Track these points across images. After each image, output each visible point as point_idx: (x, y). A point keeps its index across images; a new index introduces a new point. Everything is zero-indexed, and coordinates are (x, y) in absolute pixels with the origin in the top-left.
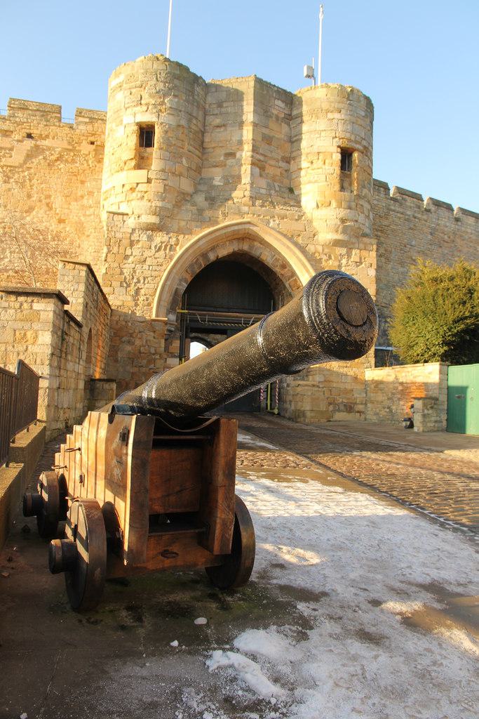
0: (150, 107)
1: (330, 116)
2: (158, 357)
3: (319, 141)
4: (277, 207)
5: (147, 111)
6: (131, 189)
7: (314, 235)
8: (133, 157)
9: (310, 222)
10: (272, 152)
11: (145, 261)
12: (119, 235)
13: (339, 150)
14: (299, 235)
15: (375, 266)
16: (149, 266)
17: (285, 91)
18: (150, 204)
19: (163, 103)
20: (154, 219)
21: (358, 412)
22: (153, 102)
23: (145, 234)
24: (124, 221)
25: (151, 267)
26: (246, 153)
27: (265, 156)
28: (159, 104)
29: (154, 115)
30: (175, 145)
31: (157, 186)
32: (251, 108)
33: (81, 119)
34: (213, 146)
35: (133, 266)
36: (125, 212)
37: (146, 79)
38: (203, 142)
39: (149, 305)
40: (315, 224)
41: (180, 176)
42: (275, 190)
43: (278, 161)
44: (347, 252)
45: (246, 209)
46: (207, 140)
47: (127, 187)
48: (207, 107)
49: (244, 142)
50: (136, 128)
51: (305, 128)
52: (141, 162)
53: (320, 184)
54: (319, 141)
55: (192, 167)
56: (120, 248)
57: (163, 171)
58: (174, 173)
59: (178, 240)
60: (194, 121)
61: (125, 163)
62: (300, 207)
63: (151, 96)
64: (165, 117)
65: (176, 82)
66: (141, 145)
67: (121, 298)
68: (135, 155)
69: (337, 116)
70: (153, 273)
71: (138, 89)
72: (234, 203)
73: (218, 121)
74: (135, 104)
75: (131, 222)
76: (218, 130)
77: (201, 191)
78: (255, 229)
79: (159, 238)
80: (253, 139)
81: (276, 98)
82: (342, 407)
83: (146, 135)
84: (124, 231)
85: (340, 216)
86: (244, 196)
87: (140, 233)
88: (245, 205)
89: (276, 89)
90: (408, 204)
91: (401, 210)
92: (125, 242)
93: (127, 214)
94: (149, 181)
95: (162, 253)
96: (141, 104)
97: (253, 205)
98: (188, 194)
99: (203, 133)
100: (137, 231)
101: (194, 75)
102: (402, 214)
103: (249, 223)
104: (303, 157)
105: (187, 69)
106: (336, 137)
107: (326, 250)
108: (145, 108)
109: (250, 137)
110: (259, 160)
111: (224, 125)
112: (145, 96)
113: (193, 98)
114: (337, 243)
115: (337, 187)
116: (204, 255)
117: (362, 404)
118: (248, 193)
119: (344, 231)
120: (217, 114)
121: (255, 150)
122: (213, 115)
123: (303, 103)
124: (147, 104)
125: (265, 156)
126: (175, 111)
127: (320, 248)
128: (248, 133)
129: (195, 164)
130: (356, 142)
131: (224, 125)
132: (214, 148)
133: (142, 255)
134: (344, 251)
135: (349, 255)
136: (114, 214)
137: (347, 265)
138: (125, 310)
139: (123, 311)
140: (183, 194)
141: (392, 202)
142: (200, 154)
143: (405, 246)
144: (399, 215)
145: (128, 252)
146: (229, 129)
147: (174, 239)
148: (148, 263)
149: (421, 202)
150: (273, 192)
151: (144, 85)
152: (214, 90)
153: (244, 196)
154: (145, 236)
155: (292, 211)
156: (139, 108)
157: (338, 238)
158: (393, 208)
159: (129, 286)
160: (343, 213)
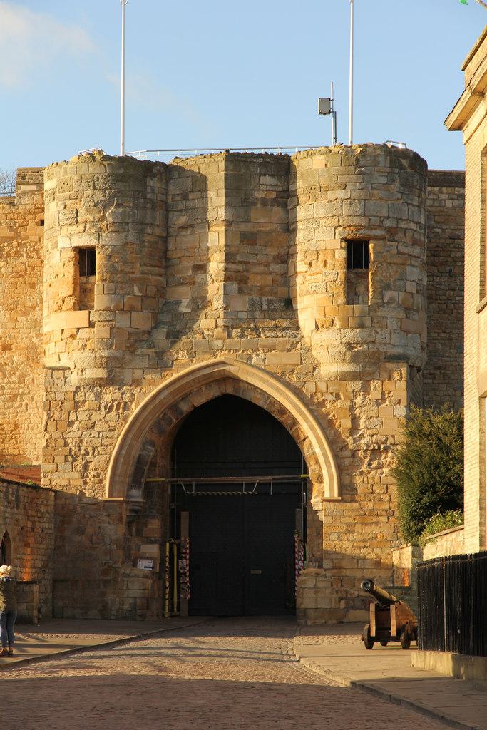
0: (88, 226)
1: (331, 195)
3: (319, 234)
4: (262, 335)
5: (84, 231)
6: (71, 336)
7: (314, 369)
8: (71, 293)
9: (308, 350)
10: (257, 255)
11: (93, 426)
12: (60, 397)
13: (344, 244)
14: (293, 371)
15: (404, 402)
16: (99, 432)
19: (103, 218)
20: (101, 373)
22: (91, 219)
23: (92, 391)
24: (66, 378)
25: (101, 434)
26: (216, 265)
28: (99, 221)
29: (92, 238)
30: (121, 271)
31: (101, 331)
32: (221, 201)
33: (24, 188)
34: (179, 255)
35: (79, 433)
36: (66, 365)
37: (81, 188)
38: (166, 251)
39: (101, 482)
40: (314, 353)
43: (267, 265)
45: (219, 343)
46: (171, 247)
47: (67, 334)
48: (170, 199)
49: (212, 249)
50: (72, 254)
51: (301, 213)
52: (82, 299)
53: (319, 296)
54: (319, 234)
55: (149, 293)
56: (63, 412)
57: (108, 309)
58: (121, 310)
59: (133, 395)
60: (149, 230)
61: (63, 301)
62: (298, 328)
63: (88, 211)
64: (108, 238)
65: (119, 185)
66: (82, 274)
67: (66, 476)
68: (74, 290)
69: (340, 194)
70: (105, 442)
71: (73, 201)
72: (203, 338)
73: (183, 220)
74: (70, 222)
75: (74, 378)
77: (164, 323)
78: (227, 368)
79: (110, 395)
80: (226, 245)
81: (261, 175)
83: (85, 258)
85: (345, 340)
86: (217, 326)
87: (86, 390)
88: (218, 339)
89: (261, 160)
92: (69, 405)
93: (69, 369)
94: (91, 325)
95: (114, 413)
96: (77, 222)
97: (229, 336)
99: (165, 240)
100: (82, 388)
103: (222, 363)
104: (299, 257)
106: (340, 226)
107: (332, 388)
108: (82, 228)
109: (222, 242)
111: (191, 226)
112: (82, 211)
114: (344, 377)
116: (174, 407)
118: (221, 322)
119: (355, 359)
120: (181, 211)
121: (229, 258)
122: (177, 211)
123: (298, 175)
124: (85, 222)
126: (120, 226)
127: (322, 386)
128: (216, 238)
130: (370, 227)
131: (191, 226)
132: (180, 258)
133: (90, 419)
134: (358, 385)
135: (366, 390)
136: (53, 369)
137: (363, 405)
138: (72, 491)
139: (71, 492)
140: (137, 334)
142: (162, 271)
145: (73, 417)
147: (129, 395)
148: (97, 429)
150: (258, 313)
151: (79, 197)
152: (176, 174)
153: (217, 326)
154: (92, 394)
155: (285, 338)
156: (74, 228)
157: (345, 370)
159: (75, 460)
160: (350, 334)
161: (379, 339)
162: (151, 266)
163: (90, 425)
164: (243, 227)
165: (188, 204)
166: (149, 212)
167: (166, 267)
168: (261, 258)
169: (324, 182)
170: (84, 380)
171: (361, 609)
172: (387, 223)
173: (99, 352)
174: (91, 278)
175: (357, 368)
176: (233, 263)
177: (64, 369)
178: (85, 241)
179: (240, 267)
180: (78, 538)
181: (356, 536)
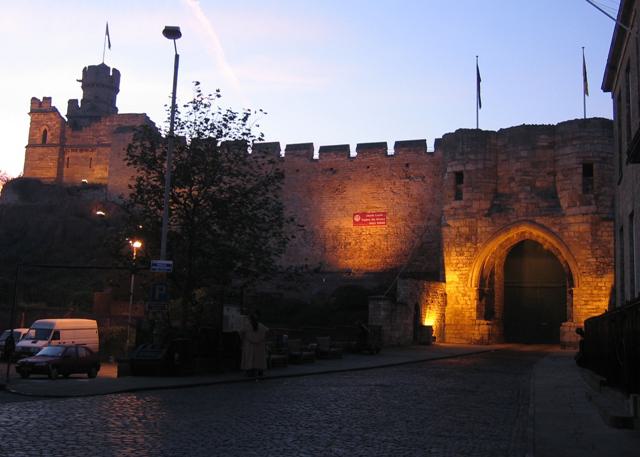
1: (574, 142)
172: (601, 155)
174: (463, 185)
178: (459, 168)
181: (589, 307)
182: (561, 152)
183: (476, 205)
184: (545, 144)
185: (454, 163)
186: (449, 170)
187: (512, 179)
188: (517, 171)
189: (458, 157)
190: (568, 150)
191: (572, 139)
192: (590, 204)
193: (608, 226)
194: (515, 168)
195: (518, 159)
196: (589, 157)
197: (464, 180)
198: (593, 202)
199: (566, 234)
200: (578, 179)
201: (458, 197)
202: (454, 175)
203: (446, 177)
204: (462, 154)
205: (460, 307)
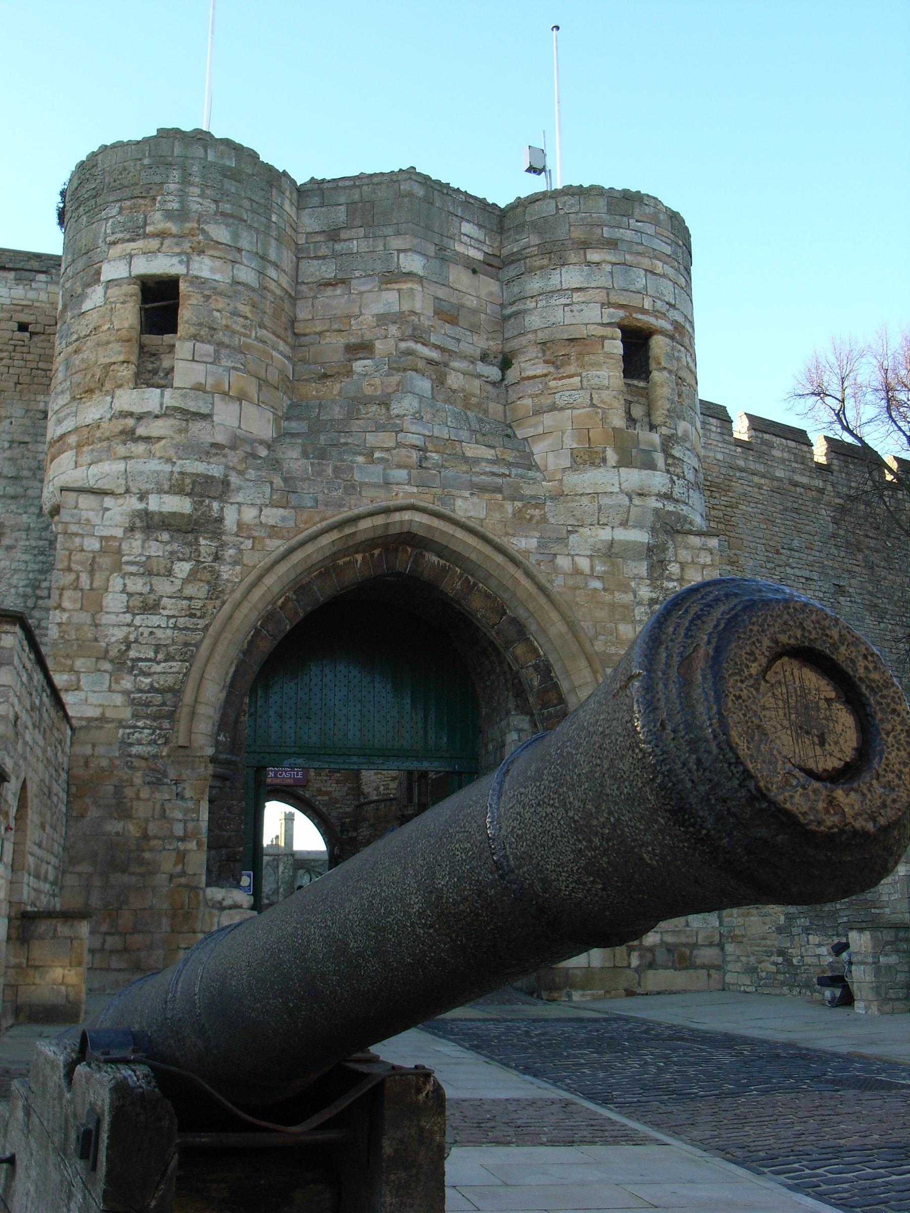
1: (594, 256)
2: (193, 845)
16: (169, 617)
17: (483, 202)
18: (167, 468)
21: (703, 967)
27: (443, 350)
29: (175, 260)
34: (318, 329)
38: (293, 321)
41: (240, 400)
42: (470, 429)
44: (651, 568)
45: (402, 474)
55: (269, 377)
56: (97, 575)
58: (226, 394)
63: (169, 215)
66: (142, 333)
76: (329, 291)
82: (661, 956)
84: (106, 533)
88: (399, 466)
90: (776, 453)
91: (761, 468)
98: (262, 442)
99: (294, 300)
101: (270, 169)
102: (763, 476)
105: (253, 156)
107: (599, 568)
110: (430, 362)
111: (343, 281)
113: (269, 219)
115: (618, 420)
117: (711, 945)
120: (324, 258)
122: (317, 258)
125: (443, 350)
127: (584, 564)
129: (277, 372)
131: (343, 281)
132: (320, 334)
141: (739, 450)
143: (778, 553)
144: (756, 479)
146: (357, 286)
149: (805, 448)
150: (464, 434)
158: (741, 463)
161: (678, 491)
162: (274, 333)
163: (151, 601)
164: (441, 292)
165: (338, 247)
166: (273, 242)
167: (293, 347)
168: (465, 348)
169: (577, 234)
170: (146, 514)
171: (666, 968)
173: (179, 462)
174: (167, 338)
175: (641, 536)
176: (424, 344)
177: (101, 493)
178: (163, 265)
179: (435, 355)
180: (114, 826)
182: (534, 284)
183: (226, 414)
184: (473, 253)
185: (140, 244)
186: (113, 270)
187: (363, 349)
188: (383, 319)
189: (157, 222)
190: (571, 277)
191: (584, 246)
192: (651, 466)
193: (704, 548)
194: (378, 308)
195: (393, 277)
196: (643, 311)
197: (185, 314)
198: (660, 459)
199: (563, 562)
200: (608, 373)
201: (150, 371)
202: (135, 289)
203: (95, 297)
204: (182, 215)
205: (133, 830)
